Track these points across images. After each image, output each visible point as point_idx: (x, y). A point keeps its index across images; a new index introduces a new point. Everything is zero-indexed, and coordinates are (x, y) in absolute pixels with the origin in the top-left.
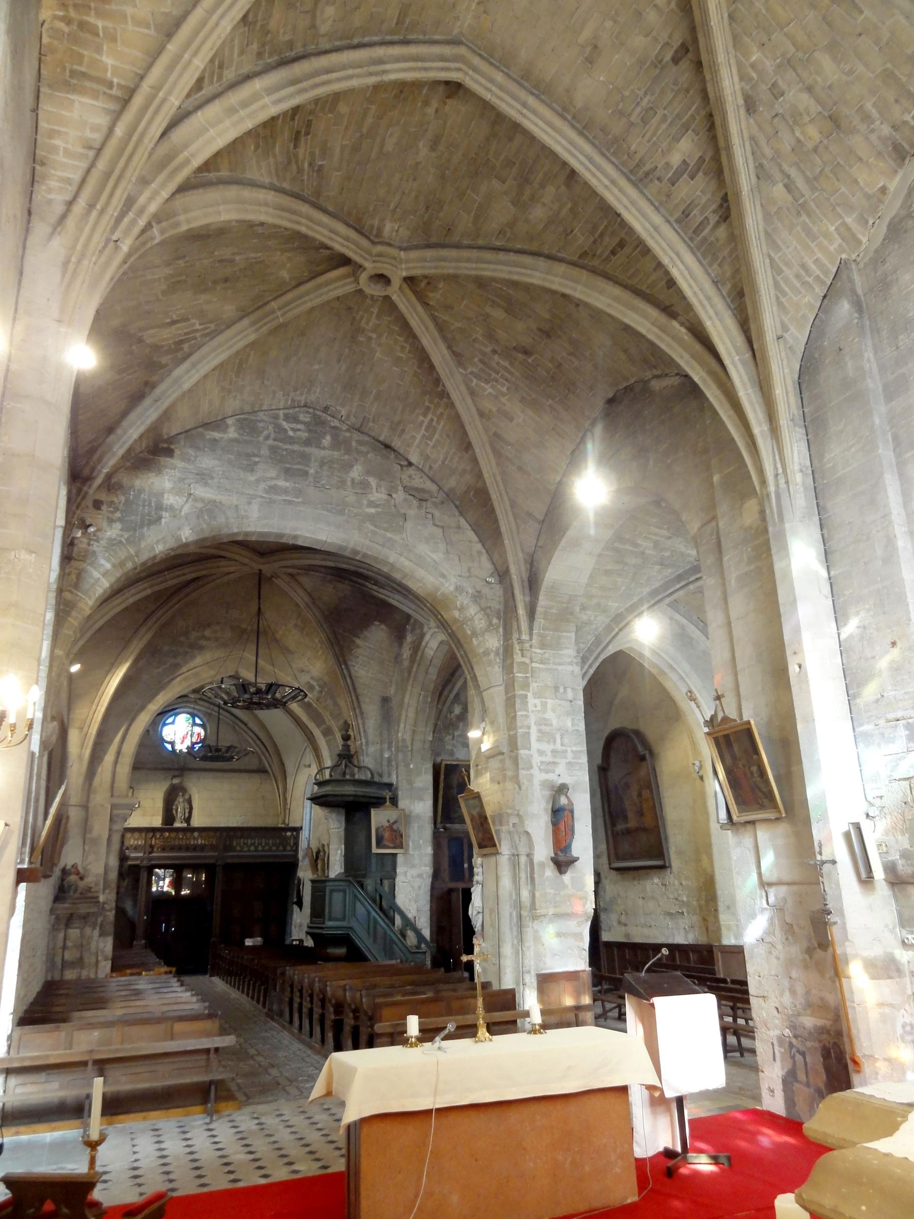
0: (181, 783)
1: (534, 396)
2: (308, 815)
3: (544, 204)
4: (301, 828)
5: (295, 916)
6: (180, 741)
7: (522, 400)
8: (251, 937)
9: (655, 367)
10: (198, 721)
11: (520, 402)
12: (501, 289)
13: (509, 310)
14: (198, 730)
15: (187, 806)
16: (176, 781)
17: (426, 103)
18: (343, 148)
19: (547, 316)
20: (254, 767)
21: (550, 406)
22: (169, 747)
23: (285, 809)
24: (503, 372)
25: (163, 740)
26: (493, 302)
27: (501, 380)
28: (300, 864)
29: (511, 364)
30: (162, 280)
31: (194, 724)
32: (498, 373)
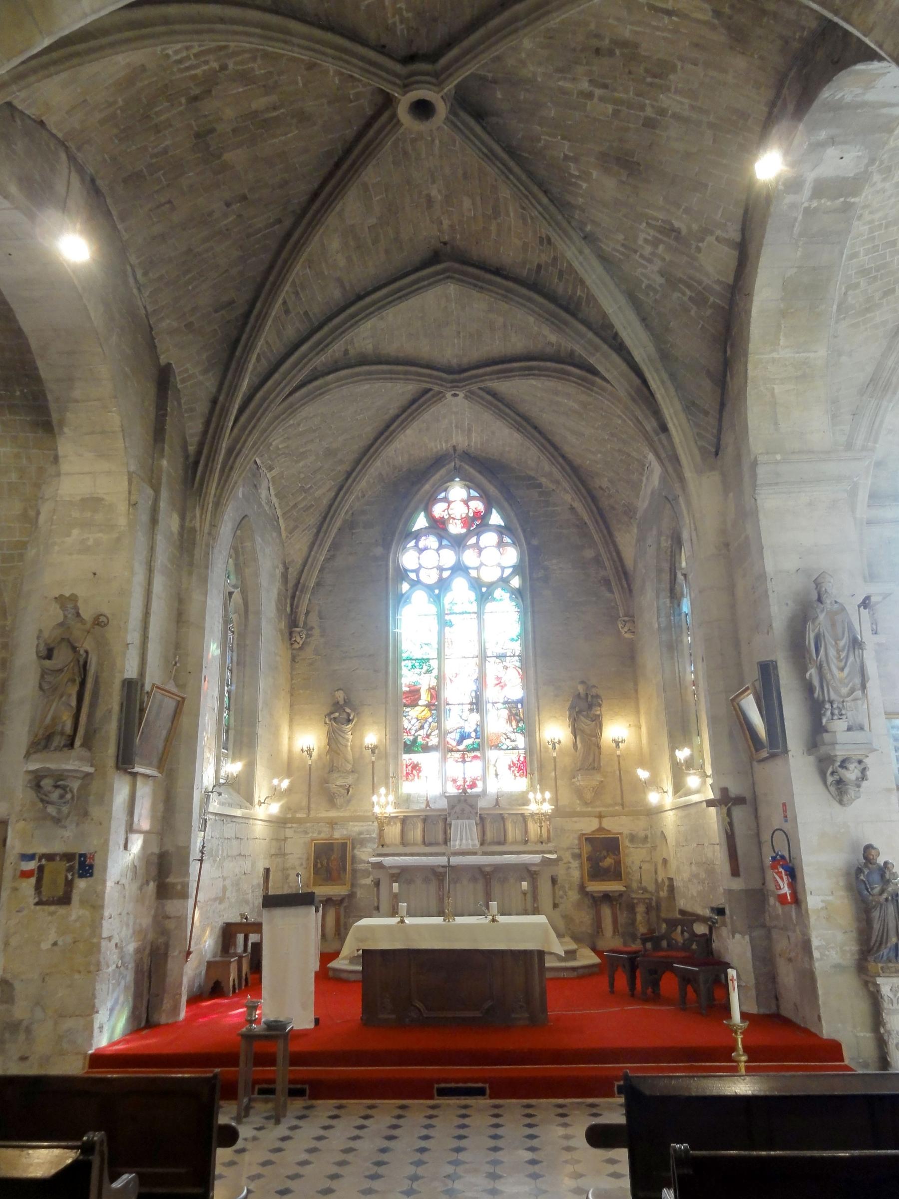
1: (139, 85)
3: (337, 252)
7: (143, 68)
9: (145, 274)
11: (143, 66)
12: (286, 134)
13: (256, 113)
17: (452, 227)
18: (508, 215)
19: (227, 156)
21: (115, 102)
24: (193, 62)
26: (275, 108)
27: (184, 54)
29: (194, 77)
30: (673, 90)
32: (196, 55)
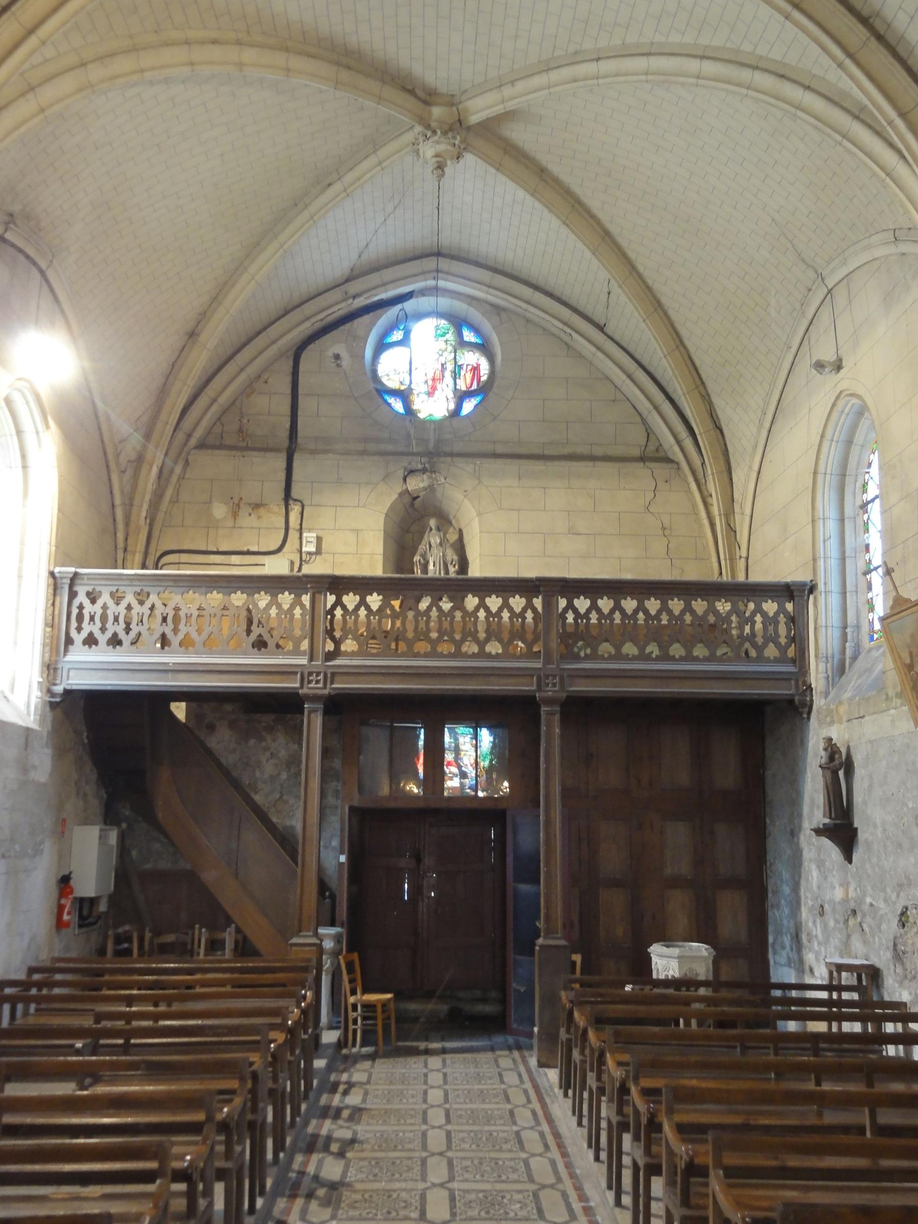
0: (431, 489)
2: (833, 544)
4: (812, 589)
5: (812, 875)
6: (424, 388)
8: (666, 938)
10: (469, 336)
14: (470, 358)
15: (451, 555)
16: (416, 484)
20: (636, 452)
22: (398, 406)
23: (732, 560)
25: (383, 391)
28: (819, 702)
31: (461, 344)
